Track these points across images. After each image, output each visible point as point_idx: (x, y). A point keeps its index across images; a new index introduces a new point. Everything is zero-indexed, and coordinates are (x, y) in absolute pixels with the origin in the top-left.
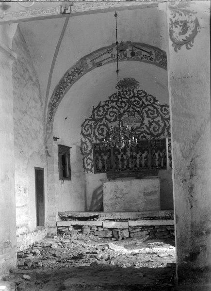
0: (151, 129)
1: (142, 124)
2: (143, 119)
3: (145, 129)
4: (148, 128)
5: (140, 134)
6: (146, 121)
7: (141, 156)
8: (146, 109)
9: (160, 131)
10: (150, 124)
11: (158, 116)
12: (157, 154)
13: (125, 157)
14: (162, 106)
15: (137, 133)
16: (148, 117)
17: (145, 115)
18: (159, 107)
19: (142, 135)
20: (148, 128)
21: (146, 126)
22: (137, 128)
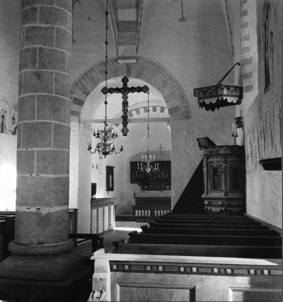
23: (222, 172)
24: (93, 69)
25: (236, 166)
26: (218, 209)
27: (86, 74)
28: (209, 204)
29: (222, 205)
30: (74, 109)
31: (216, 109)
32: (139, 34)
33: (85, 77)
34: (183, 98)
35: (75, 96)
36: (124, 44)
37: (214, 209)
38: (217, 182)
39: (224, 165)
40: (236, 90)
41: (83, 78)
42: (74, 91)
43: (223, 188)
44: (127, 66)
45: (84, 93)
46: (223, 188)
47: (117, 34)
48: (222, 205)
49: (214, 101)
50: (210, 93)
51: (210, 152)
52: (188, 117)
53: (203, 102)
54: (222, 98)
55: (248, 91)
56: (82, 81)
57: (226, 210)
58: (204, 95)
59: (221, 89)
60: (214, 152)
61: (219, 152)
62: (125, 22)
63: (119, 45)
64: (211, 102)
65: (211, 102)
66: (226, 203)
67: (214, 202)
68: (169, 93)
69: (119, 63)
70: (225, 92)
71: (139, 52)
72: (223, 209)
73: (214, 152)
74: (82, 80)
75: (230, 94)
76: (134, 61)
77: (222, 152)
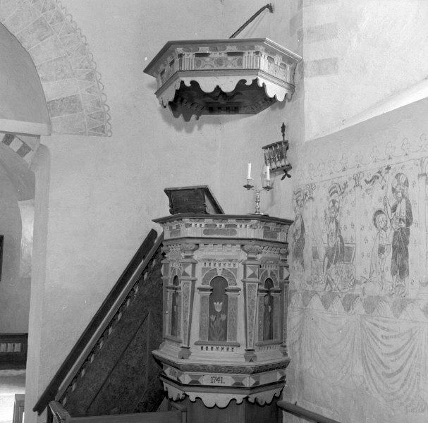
23: (238, 290)
25: (272, 273)
26: (222, 399)
28: (195, 385)
29: (238, 387)
31: (194, 117)
34: (90, 76)
37: (209, 399)
38: (223, 317)
39: (250, 272)
40: (285, 66)
43: (241, 338)
46: (241, 338)
48: (238, 387)
49: (228, 85)
50: (220, 62)
51: (206, 232)
52: (101, 130)
53: (194, 84)
54: (255, 81)
55: (320, 73)
57: (246, 399)
58: (198, 63)
59: (257, 53)
60: (218, 232)
61: (235, 232)
64: (218, 88)
65: (218, 88)
66: (249, 381)
67: (206, 379)
68: (54, 57)
70: (264, 64)
72: (239, 398)
73: (218, 232)
75: (271, 73)
77: (244, 231)
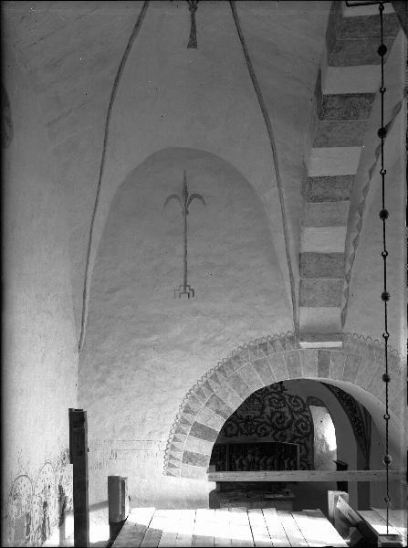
0: (274, 420)
1: (262, 413)
2: (264, 407)
3: (266, 419)
4: (270, 419)
5: (258, 426)
6: (268, 410)
7: (265, 462)
8: (269, 397)
9: (285, 425)
10: (273, 414)
11: (284, 406)
12: (286, 462)
13: (244, 462)
14: (291, 397)
15: (255, 423)
16: (271, 405)
17: (267, 402)
18: (287, 397)
19: (261, 426)
20: (270, 419)
21: (268, 417)
22: (255, 417)
24: (236, 357)
27: (220, 369)
30: (194, 450)
32: (348, 282)
33: (221, 376)
35: (198, 419)
36: (312, 304)
41: (214, 377)
42: (194, 406)
44: (319, 352)
45: (218, 412)
47: (297, 279)
56: (212, 383)
62: (319, 256)
63: (301, 305)
69: (299, 346)
71: (346, 326)
74: (212, 383)
76: (339, 344)
